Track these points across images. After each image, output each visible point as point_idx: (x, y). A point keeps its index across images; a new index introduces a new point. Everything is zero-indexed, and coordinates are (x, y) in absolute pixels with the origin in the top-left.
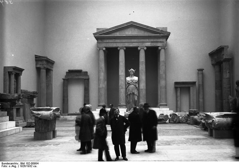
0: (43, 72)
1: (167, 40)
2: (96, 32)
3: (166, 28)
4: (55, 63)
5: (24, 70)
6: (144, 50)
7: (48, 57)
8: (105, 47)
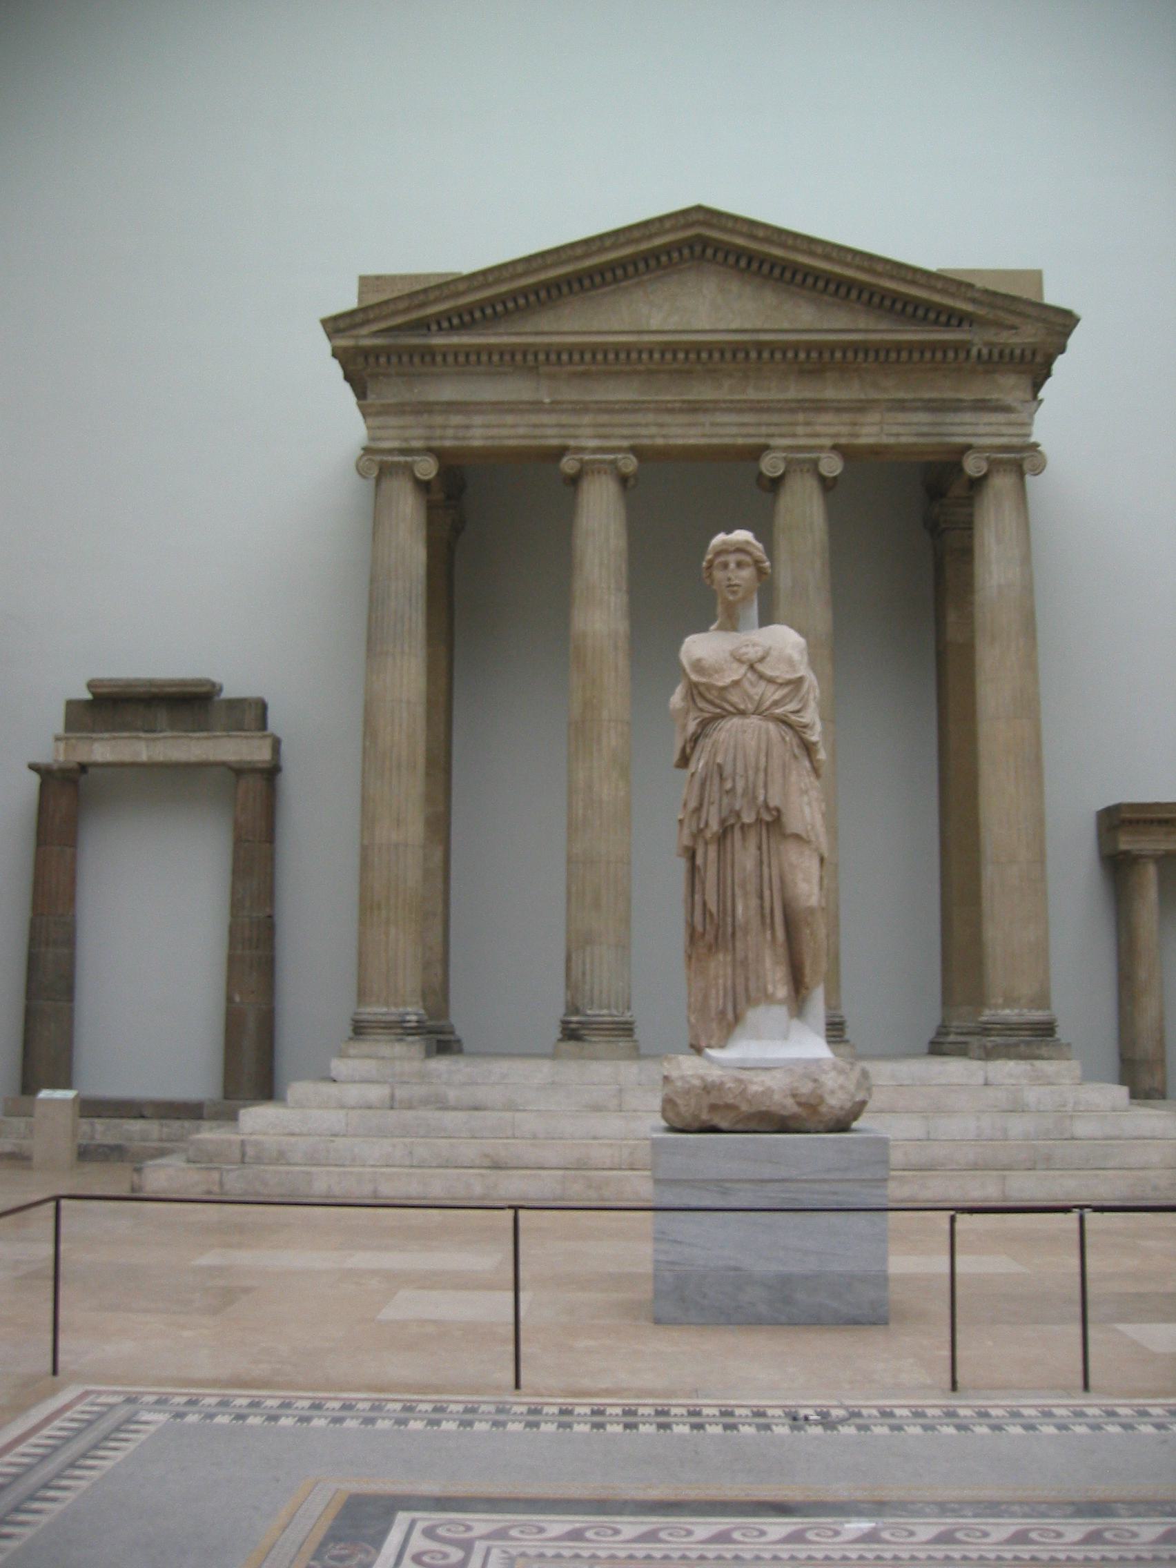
2: (348, 301)
3: (1035, 277)
6: (822, 479)
8: (430, 451)
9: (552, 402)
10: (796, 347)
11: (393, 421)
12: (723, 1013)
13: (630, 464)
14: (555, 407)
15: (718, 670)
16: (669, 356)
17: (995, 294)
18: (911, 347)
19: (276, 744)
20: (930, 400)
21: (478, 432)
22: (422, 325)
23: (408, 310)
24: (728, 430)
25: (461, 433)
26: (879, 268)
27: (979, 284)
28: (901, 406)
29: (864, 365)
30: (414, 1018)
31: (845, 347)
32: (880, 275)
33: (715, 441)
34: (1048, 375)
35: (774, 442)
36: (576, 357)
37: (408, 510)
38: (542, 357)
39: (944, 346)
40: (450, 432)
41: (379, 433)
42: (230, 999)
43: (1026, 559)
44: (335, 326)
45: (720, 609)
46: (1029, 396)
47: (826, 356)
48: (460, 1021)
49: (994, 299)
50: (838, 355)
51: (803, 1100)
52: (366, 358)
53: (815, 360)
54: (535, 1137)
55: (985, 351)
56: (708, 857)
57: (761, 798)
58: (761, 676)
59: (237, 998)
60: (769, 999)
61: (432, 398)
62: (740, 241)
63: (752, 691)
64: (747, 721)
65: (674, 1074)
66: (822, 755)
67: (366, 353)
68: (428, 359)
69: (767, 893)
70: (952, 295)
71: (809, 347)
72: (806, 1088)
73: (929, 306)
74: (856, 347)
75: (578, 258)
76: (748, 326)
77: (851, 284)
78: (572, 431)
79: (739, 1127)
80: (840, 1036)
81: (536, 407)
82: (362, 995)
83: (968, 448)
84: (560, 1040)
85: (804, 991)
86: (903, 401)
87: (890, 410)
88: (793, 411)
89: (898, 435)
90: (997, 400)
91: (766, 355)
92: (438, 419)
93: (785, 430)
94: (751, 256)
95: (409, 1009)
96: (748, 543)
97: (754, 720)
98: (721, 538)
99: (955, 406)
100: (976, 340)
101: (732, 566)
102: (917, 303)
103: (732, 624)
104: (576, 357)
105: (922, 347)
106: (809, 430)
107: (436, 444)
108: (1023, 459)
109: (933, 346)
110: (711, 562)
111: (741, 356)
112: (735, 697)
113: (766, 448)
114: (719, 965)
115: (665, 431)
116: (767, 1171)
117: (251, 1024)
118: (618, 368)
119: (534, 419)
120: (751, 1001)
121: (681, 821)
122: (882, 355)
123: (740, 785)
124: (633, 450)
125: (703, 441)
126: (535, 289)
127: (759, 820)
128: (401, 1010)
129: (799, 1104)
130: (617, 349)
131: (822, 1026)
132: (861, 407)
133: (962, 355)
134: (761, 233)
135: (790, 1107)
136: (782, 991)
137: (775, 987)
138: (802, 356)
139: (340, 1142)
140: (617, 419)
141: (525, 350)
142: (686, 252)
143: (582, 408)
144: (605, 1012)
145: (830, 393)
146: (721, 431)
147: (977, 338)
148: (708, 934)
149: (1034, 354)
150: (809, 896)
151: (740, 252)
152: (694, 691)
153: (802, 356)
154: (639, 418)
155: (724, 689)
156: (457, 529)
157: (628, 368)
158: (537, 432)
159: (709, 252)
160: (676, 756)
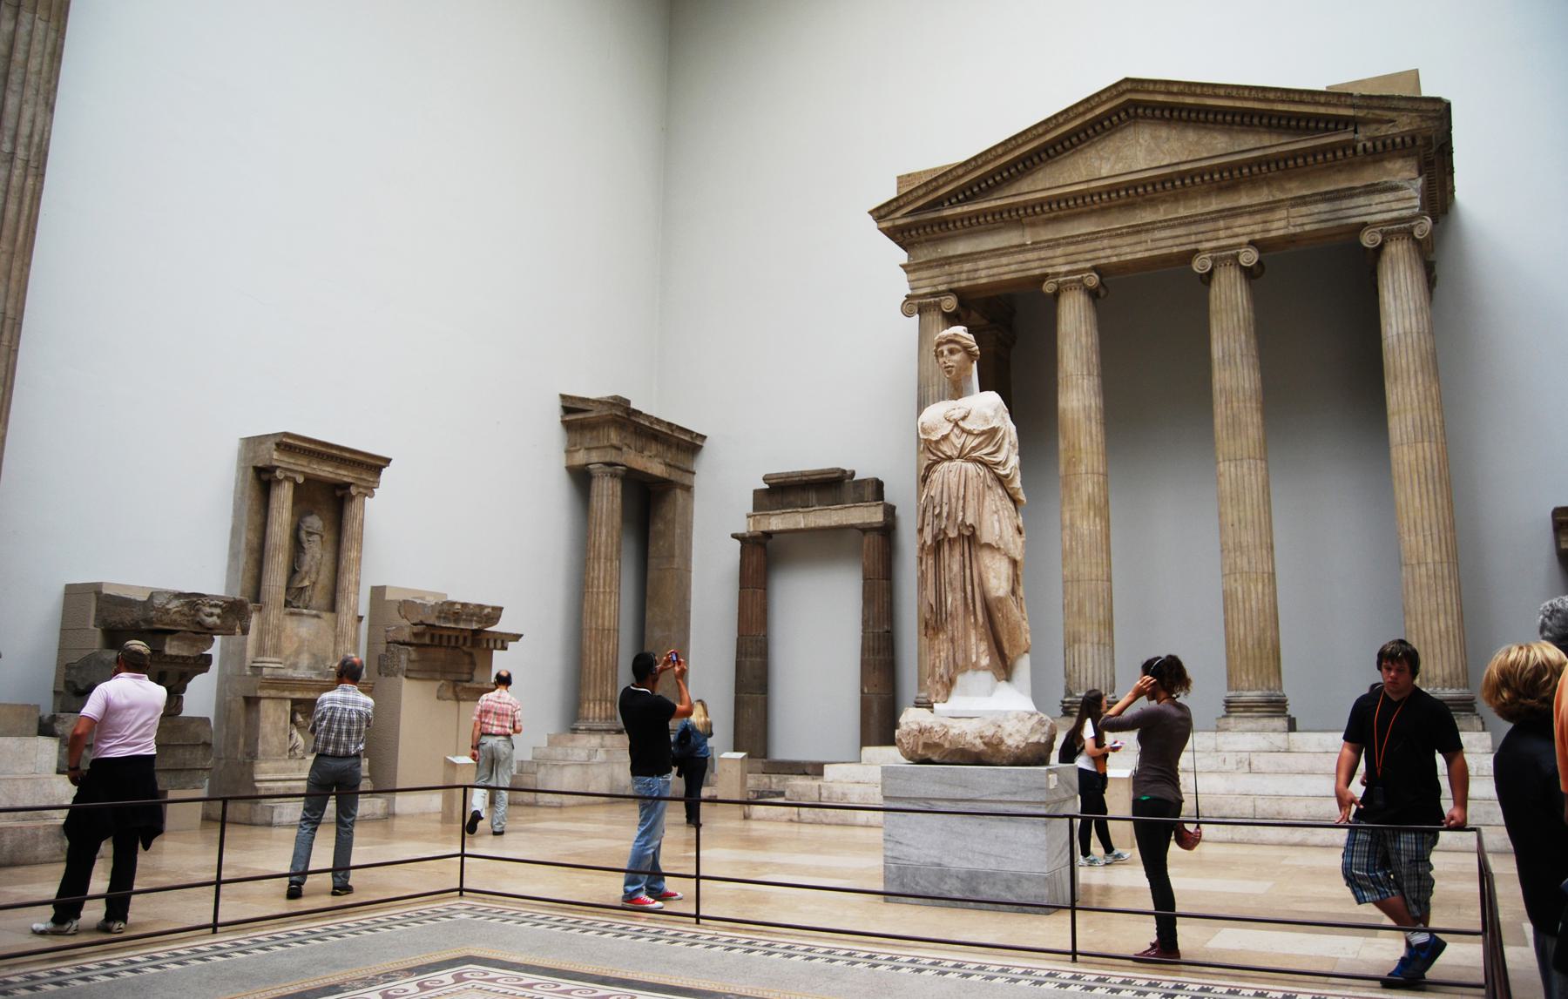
0: (608, 494)
3: (1415, 75)
4: (706, 445)
5: (388, 461)
6: (1243, 269)
7: (633, 406)
8: (951, 291)
10: (1210, 170)
11: (925, 274)
14: (1036, 246)
17: (1371, 97)
18: (1304, 153)
19: (890, 511)
21: (983, 273)
22: (937, 204)
23: (925, 195)
25: (972, 275)
26: (1271, 96)
27: (1356, 93)
28: (1302, 201)
31: (1249, 163)
32: (1273, 101)
33: (1156, 253)
35: (1200, 247)
40: (964, 276)
44: (880, 214)
47: (1236, 173)
49: (1369, 101)
50: (1245, 171)
53: (1227, 177)
55: (1369, 144)
58: (963, 431)
60: (976, 667)
62: (1160, 98)
69: (969, 588)
70: (1335, 105)
71: (1220, 168)
72: (989, 733)
73: (1318, 118)
74: (1259, 162)
75: (1040, 136)
81: (1022, 248)
83: (1365, 224)
87: (1293, 206)
91: (1187, 181)
92: (956, 268)
93: (1209, 235)
94: (1171, 107)
97: (958, 462)
99: (1350, 193)
102: (1308, 117)
105: (1314, 151)
106: (1229, 232)
107: (955, 285)
109: (1323, 149)
111: (1168, 185)
112: (945, 447)
113: (1197, 251)
115: (1117, 251)
116: (959, 793)
119: (1021, 257)
120: (964, 671)
122: (1282, 165)
123: (945, 509)
124: (1095, 269)
125: (1147, 254)
126: (1013, 163)
127: (961, 535)
130: (1075, 196)
131: (1027, 686)
132: (1271, 207)
133: (1349, 152)
134: (1175, 89)
135: (979, 745)
136: (985, 661)
138: (1216, 176)
140: (1081, 247)
142: (1122, 115)
143: (1054, 244)
145: (1244, 199)
146: (1163, 244)
149: (1414, 140)
151: (1163, 106)
153: (1216, 176)
154: (1097, 244)
155: (937, 442)
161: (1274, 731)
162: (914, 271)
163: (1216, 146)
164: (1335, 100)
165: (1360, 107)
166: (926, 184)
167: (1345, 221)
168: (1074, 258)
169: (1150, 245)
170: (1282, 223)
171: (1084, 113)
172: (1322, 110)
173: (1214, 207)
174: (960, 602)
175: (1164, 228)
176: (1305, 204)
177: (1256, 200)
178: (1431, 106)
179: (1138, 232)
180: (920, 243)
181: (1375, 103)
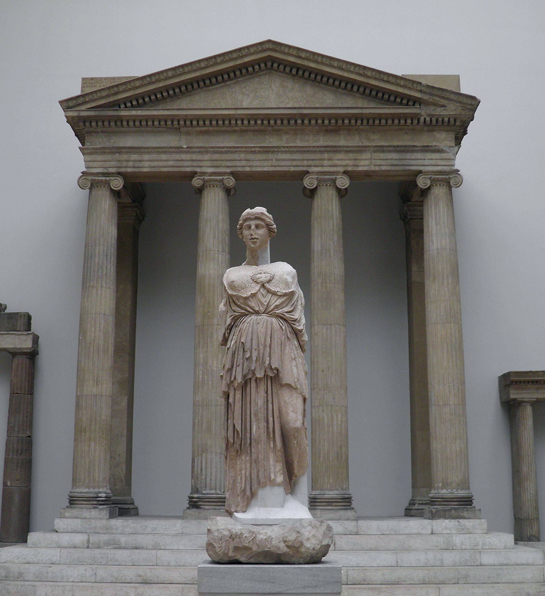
1: (458, 141)
2: (75, 90)
3: (456, 79)
6: (339, 190)
8: (119, 174)
9: (187, 148)
10: (323, 117)
12: (244, 491)
13: (231, 182)
15: (244, 287)
16: (252, 122)
17: (433, 87)
18: (387, 117)
19: (36, 339)
20: (398, 146)
21: (147, 164)
22: (116, 105)
23: (108, 96)
24: (283, 163)
25: (137, 164)
26: (369, 73)
27: (424, 82)
28: (381, 149)
29: (361, 127)
30: (104, 495)
31: (350, 117)
33: (278, 169)
34: (465, 133)
35: (310, 169)
36: (201, 123)
37: (107, 207)
38: (182, 123)
39: (405, 117)
40: (131, 164)
41: (91, 164)
42: (5, 484)
43: (453, 233)
44: (68, 104)
45: (248, 253)
46: (453, 144)
47: (340, 122)
48: (138, 495)
50: (346, 121)
51: (290, 544)
52: (84, 123)
53: (334, 124)
54: (169, 565)
55: (428, 119)
56: (236, 397)
57: (267, 362)
58: (269, 291)
59: (9, 484)
60: (273, 483)
61: (121, 145)
63: (263, 300)
64: (260, 317)
65: (213, 528)
66: (306, 338)
67: (84, 120)
68: (119, 123)
69: (271, 419)
71: (330, 117)
72: (292, 537)
73: (397, 95)
74: (357, 117)
75: (202, 69)
76: (297, 106)
77: (353, 83)
78: (199, 163)
79: (252, 560)
80: (350, 506)
81: (178, 150)
82: (75, 481)
83: (420, 172)
84: (188, 508)
85: (294, 478)
86: (383, 146)
87: (375, 152)
88: (321, 152)
89: (380, 165)
90: (436, 146)
91: (306, 122)
92: (125, 157)
93: (317, 163)
95: (101, 490)
96: (262, 214)
97: (264, 317)
98: (248, 210)
99: (411, 149)
100: (423, 113)
101: (253, 227)
102: (391, 93)
103: (255, 261)
104: (201, 123)
105: (393, 117)
106: (330, 163)
107: (123, 170)
108: (450, 178)
109: (399, 117)
110: (241, 225)
111: (292, 122)
112: (253, 303)
113: (308, 172)
114: (243, 463)
115: (250, 164)
117: (16, 499)
118: (224, 128)
119: (178, 157)
120: (261, 485)
121: (222, 376)
122: (371, 122)
123: (255, 354)
124: (232, 173)
125: (272, 169)
126: (178, 85)
127: (266, 376)
128: (96, 490)
129: (288, 547)
130: (224, 118)
131: (306, 500)
132: (361, 150)
133: (415, 122)
134: (303, 55)
135: (283, 548)
136: (280, 479)
137: (275, 475)
138: (326, 122)
139: (54, 568)
141: (173, 119)
142: (263, 65)
143: (204, 150)
144: (213, 491)
145: (342, 141)
147: (424, 112)
148: (237, 444)
150: (296, 421)
151: (292, 65)
152: (232, 300)
153: (326, 122)
154: (236, 156)
155: (246, 298)
156: (140, 219)
157: (229, 129)
158: (180, 164)
159: (275, 65)
160: (221, 338)
161: (348, 519)
162: (91, 154)
163: (326, 101)
164: (410, 85)
165: (425, 93)
166: (109, 88)
167: (408, 168)
168: (218, 163)
169: (274, 163)
170: (367, 162)
171: (236, 59)
172: (401, 90)
173: (321, 143)
174: (263, 430)
175: (286, 152)
176: (383, 151)
177: (350, 144)
178: (469, 101)
179: (267, 152)
180: (97, 133)
181: (435, 92)
